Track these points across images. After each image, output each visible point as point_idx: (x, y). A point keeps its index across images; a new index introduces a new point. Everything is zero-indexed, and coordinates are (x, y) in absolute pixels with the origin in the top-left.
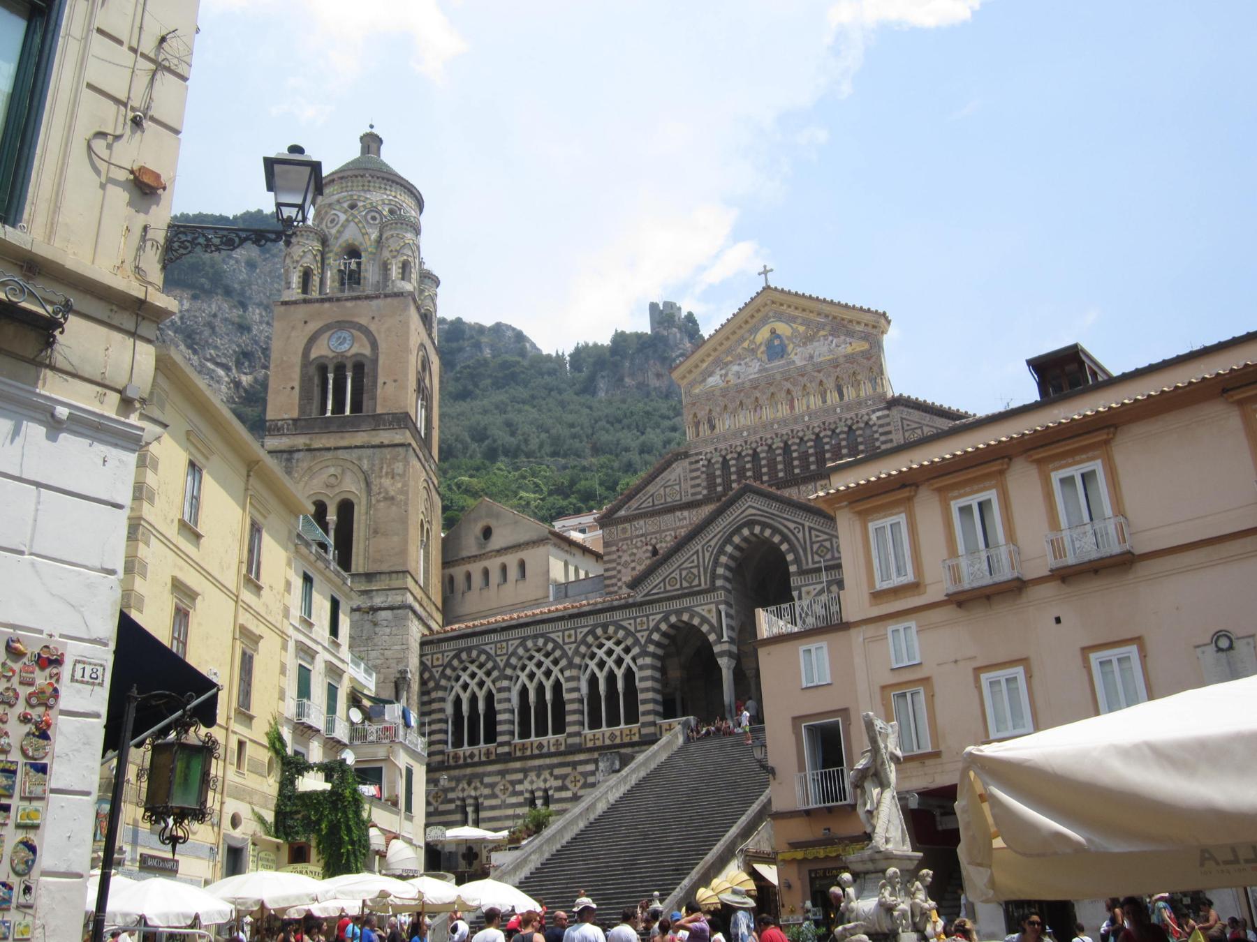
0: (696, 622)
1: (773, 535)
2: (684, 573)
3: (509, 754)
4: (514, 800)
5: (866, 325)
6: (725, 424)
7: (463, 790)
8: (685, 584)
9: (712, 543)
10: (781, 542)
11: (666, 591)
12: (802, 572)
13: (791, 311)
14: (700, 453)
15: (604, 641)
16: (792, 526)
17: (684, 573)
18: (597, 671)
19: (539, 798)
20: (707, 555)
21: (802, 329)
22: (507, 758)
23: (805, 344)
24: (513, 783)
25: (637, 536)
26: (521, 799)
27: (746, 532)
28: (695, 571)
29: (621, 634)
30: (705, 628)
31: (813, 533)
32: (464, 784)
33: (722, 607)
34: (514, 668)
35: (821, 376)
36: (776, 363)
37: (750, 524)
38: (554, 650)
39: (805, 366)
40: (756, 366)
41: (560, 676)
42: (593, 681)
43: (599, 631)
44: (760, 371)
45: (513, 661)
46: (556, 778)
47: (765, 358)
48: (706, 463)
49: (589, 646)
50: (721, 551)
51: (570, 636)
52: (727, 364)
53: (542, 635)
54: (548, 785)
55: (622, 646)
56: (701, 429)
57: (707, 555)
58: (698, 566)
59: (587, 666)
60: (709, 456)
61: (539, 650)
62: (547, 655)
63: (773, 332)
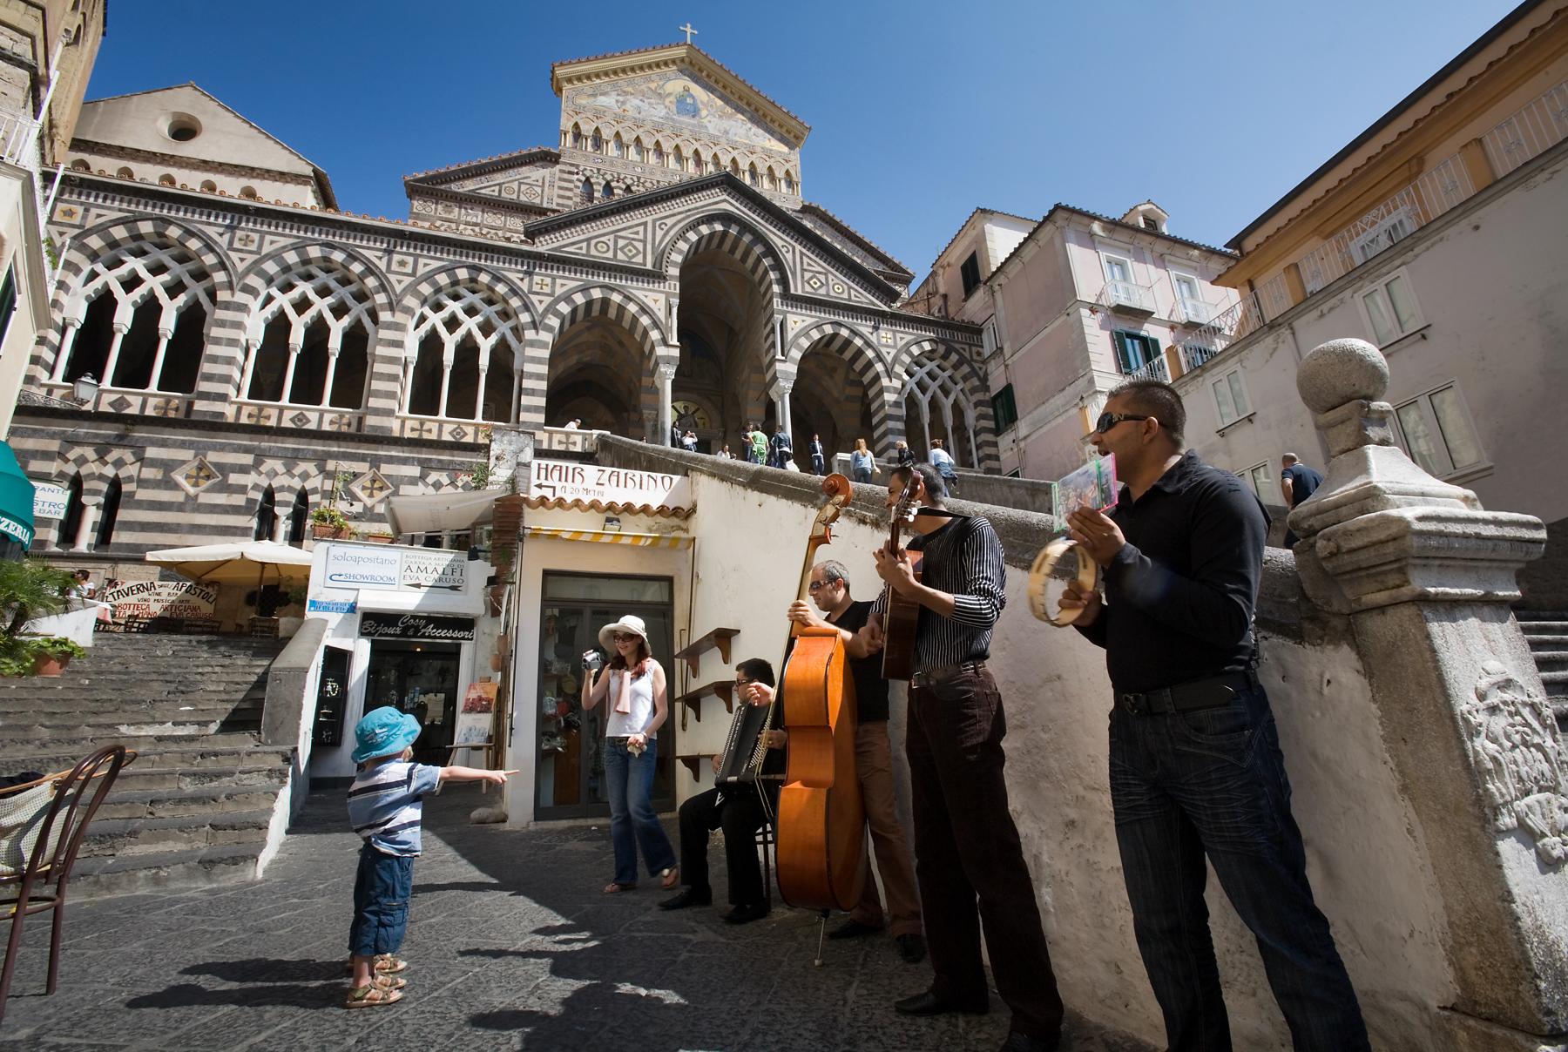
0: (632, 308)
2: (621, 243)
3: (222, 414)
4: (221, 499)
5: (789, 132)
7: (81, 461)
8: (620, 256)
9: (670, 222)
10: (765, 255)
11: (588, 254)
12: (787, 296)
14: (577, 166)
15: (462, 291)
17: (621, 243)
18: (442, 331)
19: (286, 504)
20: (659, 233)
22: (215, 425)
24: (224, 469)
25: (467, 223)
26: (239, 500)
27: (719, 227)
28: (640, 246)
29: (501, 289)
30: (645, 320)
31: (805, 260)
32: (90, 453)
33: (675, 301)
34: (270, 281)
36: (686, 119)
37: (726, 218)
38: (362, 277)
40: (663, 112)
41: (367, 321)
42: (431, 345)
43: (462, 274)
45: (271, 267)
46: (330, 475)
47: (674, 108)
49: (438, 290)
50: (682, 235)
51: (402, 263)
53: (342, 248)
54: (309, 485)
55: (497, 307)
57: (659, 233)
58: (644, 242)
59: (423, 319)
60: (588, 173)
61: (328, 271)
62: (345, 281)
63: (686, 90)
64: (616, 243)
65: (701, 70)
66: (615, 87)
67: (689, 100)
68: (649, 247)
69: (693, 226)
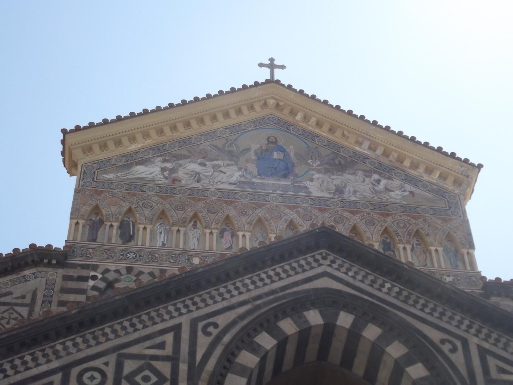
1: (386, 338)
2: (129, 366)
6: (152, 237)
9: (222, 320)
13: (311, 127)
14: (95, 268)
16: (435, 335)
17: (129, 366)
20: (203, 343)
21: (325, 152)
23: (327, 171)
27: (314, 318)
35: (356, 219)
36: (271, 181)
37: (330, 301)
39: (326, 199)
44: (240, 183)
47: (252, 168)
48: (102, 285)
50: (245, 340)
52: (178, 157)
56: (103, 235)
57: (203, 343)
58: (174, 359)
60: (111, 276)
64: (119, 366)
65: (293, 113)
66: (160, 150)
67: (276, 155)
68: (183, 367)
69: (267, 322)
